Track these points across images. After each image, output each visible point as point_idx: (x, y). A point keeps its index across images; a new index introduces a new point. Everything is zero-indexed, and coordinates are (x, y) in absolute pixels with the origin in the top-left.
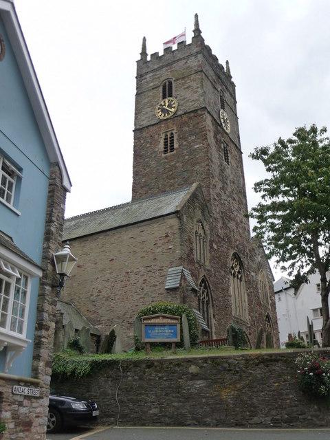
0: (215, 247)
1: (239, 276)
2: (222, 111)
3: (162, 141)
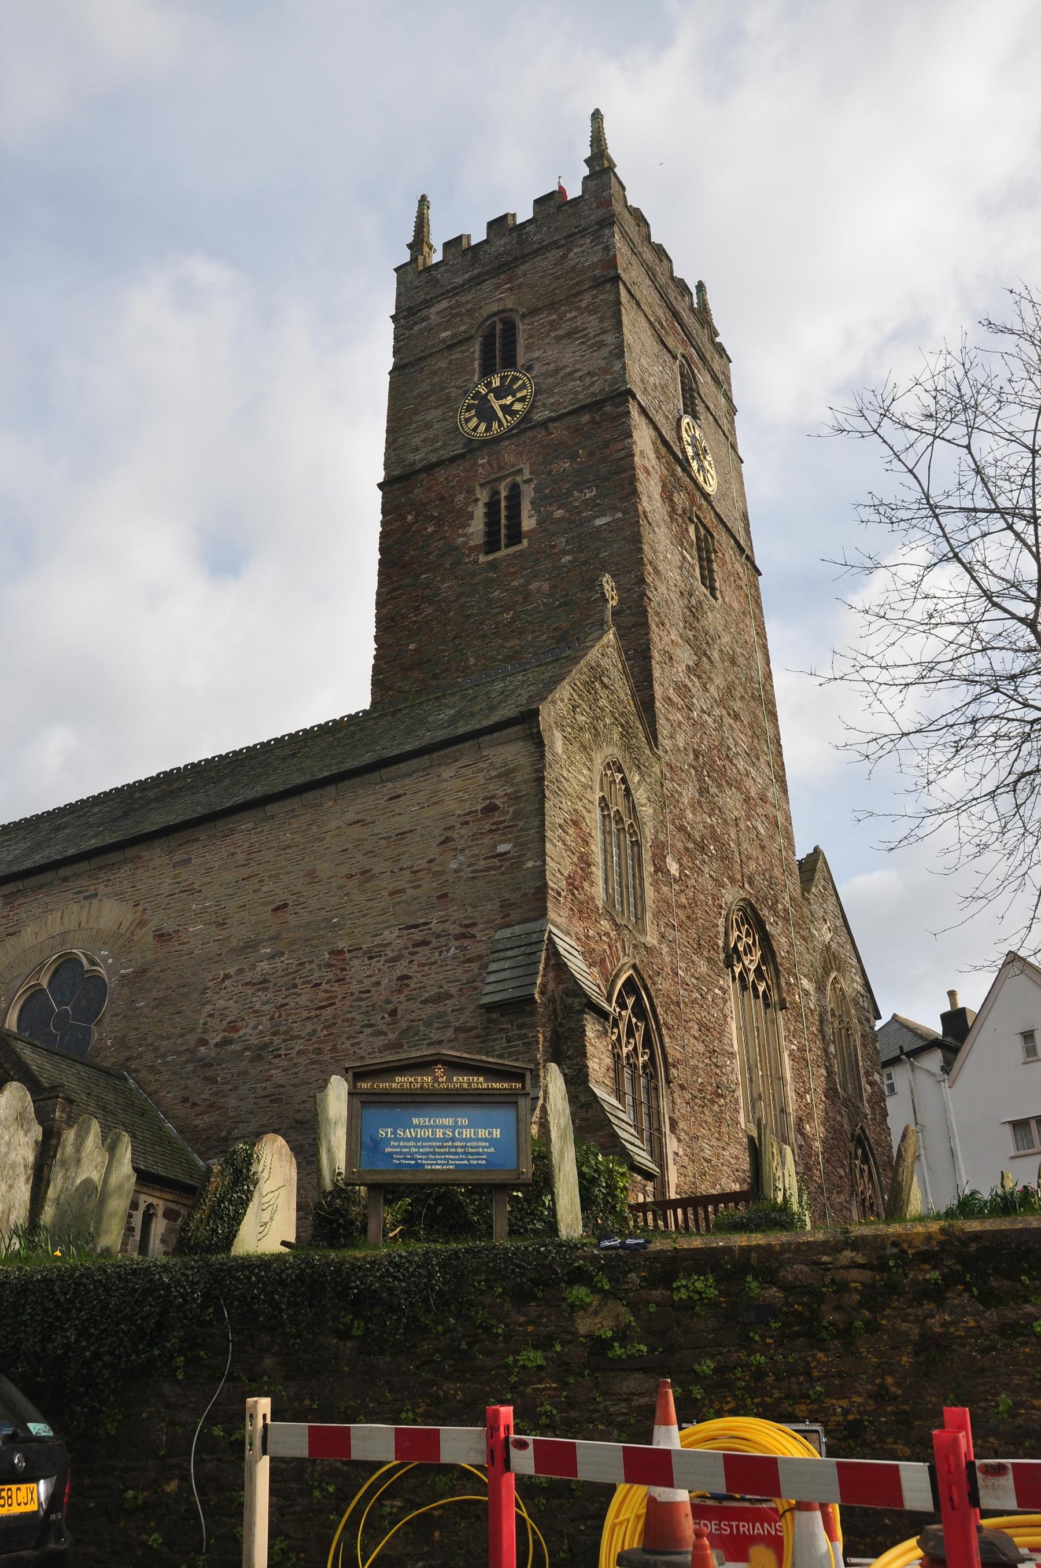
0: (674, 868)
1: (761, 988)
2: (686, 420)
3: (479, 511)
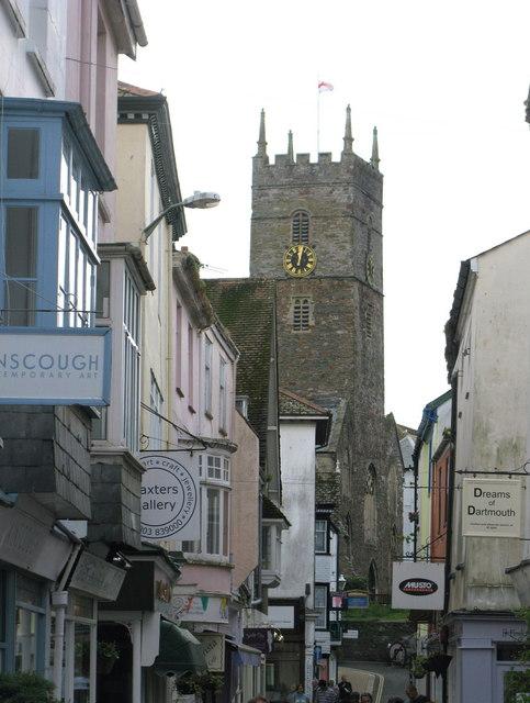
3: (292, 309)
